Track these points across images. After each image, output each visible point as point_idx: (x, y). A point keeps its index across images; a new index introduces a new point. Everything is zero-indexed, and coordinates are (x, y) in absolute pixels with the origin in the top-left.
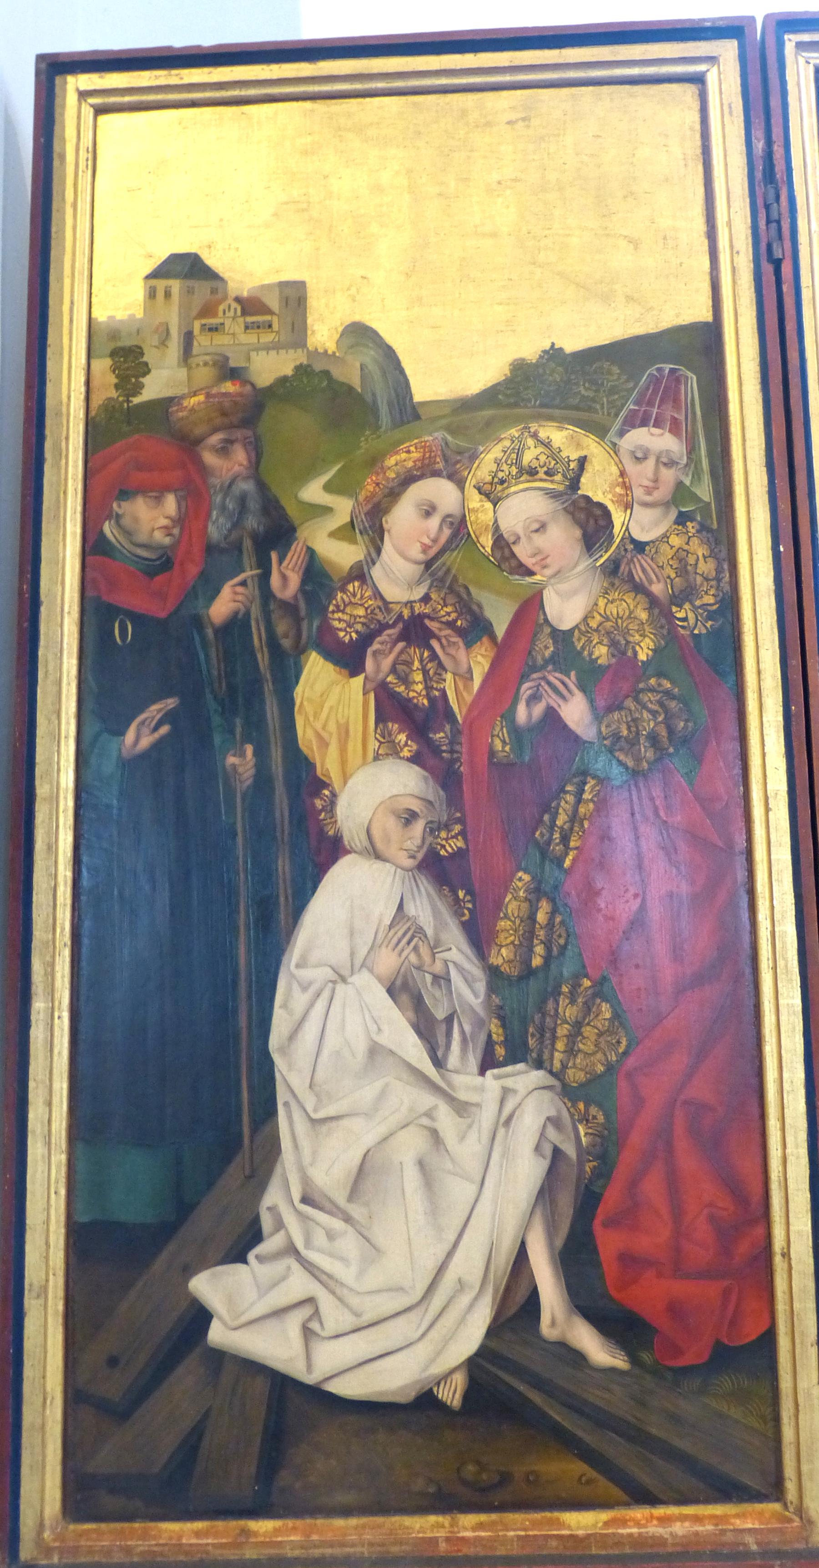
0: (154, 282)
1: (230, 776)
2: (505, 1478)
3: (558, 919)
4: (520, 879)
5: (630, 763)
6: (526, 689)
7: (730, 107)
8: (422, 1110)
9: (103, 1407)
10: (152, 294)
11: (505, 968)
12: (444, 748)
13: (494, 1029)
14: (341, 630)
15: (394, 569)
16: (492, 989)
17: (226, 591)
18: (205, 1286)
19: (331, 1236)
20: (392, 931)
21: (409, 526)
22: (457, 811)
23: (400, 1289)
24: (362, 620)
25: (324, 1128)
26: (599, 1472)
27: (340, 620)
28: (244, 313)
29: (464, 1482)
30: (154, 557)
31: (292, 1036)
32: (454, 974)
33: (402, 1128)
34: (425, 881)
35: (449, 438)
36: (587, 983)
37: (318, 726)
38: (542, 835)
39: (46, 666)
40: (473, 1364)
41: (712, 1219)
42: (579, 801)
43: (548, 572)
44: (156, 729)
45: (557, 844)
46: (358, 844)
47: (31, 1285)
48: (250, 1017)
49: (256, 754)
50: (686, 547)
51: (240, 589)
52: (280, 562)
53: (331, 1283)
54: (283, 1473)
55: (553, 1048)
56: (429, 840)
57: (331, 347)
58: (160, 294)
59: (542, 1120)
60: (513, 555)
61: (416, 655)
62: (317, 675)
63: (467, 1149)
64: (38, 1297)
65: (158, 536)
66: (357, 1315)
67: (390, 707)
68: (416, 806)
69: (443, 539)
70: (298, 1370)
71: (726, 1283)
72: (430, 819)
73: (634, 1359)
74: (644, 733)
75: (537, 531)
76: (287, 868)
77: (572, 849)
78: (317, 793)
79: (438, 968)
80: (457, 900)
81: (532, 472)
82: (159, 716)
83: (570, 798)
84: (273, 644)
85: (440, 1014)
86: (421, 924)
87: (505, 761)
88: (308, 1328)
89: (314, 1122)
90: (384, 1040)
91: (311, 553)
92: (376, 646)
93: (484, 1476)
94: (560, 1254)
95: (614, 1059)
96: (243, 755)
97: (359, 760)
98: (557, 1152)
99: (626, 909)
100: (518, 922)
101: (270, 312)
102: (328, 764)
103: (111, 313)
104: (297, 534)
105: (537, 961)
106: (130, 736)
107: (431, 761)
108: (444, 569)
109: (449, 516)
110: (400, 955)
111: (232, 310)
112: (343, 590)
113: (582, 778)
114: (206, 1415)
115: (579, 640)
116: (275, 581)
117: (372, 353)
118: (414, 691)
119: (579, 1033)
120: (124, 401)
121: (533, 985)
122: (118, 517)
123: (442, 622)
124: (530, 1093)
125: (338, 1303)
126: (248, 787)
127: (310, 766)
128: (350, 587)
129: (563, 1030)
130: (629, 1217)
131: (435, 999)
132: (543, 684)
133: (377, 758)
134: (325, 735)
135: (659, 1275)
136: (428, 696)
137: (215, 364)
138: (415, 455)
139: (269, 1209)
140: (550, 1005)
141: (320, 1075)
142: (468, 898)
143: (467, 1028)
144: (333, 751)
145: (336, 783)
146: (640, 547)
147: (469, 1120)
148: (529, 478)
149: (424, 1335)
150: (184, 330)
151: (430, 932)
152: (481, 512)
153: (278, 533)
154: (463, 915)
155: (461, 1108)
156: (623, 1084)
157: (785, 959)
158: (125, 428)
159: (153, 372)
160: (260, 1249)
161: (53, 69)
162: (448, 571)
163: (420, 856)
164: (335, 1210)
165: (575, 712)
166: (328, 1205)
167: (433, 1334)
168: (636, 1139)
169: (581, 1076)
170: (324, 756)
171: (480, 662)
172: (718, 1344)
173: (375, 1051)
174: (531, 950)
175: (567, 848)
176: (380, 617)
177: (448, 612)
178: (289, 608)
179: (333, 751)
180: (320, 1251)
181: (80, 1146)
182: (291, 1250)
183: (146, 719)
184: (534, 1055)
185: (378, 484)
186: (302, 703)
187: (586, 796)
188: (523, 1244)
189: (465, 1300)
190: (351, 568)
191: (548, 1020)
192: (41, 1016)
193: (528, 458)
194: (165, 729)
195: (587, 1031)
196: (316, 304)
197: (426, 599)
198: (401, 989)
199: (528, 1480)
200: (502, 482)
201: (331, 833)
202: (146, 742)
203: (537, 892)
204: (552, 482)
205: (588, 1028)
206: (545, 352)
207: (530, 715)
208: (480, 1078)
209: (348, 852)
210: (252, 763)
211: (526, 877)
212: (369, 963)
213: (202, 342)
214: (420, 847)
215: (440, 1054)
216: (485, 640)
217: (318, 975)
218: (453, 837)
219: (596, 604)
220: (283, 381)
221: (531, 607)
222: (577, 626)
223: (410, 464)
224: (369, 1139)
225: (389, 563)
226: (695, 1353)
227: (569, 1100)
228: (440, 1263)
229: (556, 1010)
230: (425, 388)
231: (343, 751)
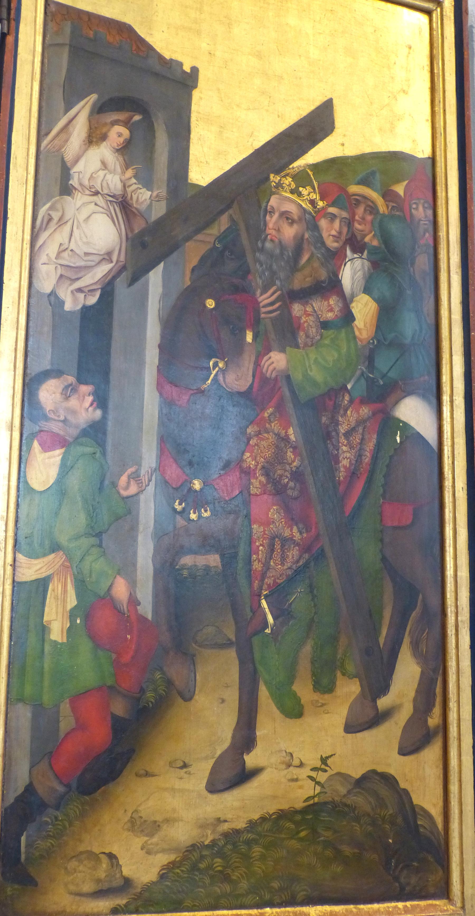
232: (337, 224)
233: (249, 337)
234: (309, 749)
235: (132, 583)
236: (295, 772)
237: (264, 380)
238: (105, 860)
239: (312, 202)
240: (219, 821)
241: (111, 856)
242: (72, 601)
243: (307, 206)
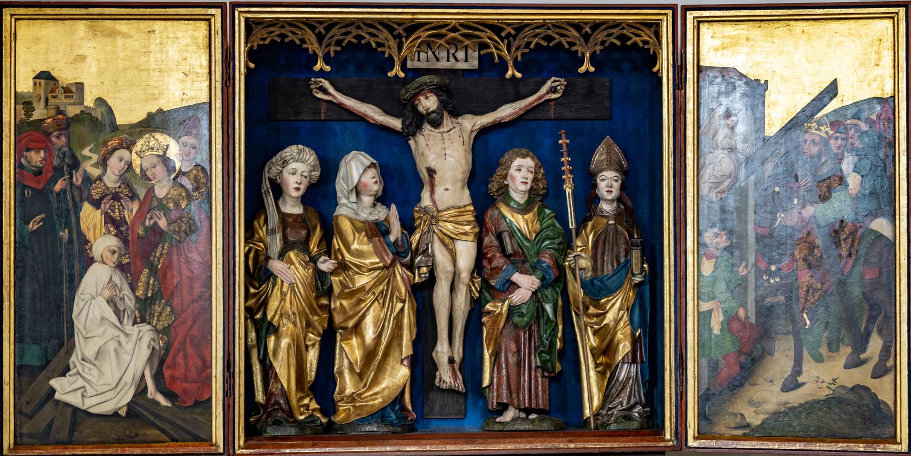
2: (137, 435)
10: (35, 84)
18: (53, 383)
19: (90, 370)
21: (115, 164)
40: (129, 405)
57: (92, 105)
61: (116, 203)
62: (87, 209)
63: (128, 346)
68: (116, 249)
70: (80, 406)
81: (152, 149)
84: (73, 199)
90: (105, 316)
91: (85, 171)
106: (31, 225)
116: (74, 179)
146: (184, 174)
152: (136, 161)
153: (75, 164)
155: (127, 335)
173: (103, 319)
182: (78, 373)
198: (111, 301)
202: (35, 227)
213: (51, 101)
217: (87, 297)
221: (151, 191)
224: (101, 343)
226: (190, 403)
232: (839, 141)
233: (796, 201)
234: (827, 375)
235: (746, 311)
236: (820, 385)
237: (803, 219)
238: (739, 416)
239: (827, 133)
240: (786, 403)
241: (742, 415)
242: (722, 318)
243: (824, 135)
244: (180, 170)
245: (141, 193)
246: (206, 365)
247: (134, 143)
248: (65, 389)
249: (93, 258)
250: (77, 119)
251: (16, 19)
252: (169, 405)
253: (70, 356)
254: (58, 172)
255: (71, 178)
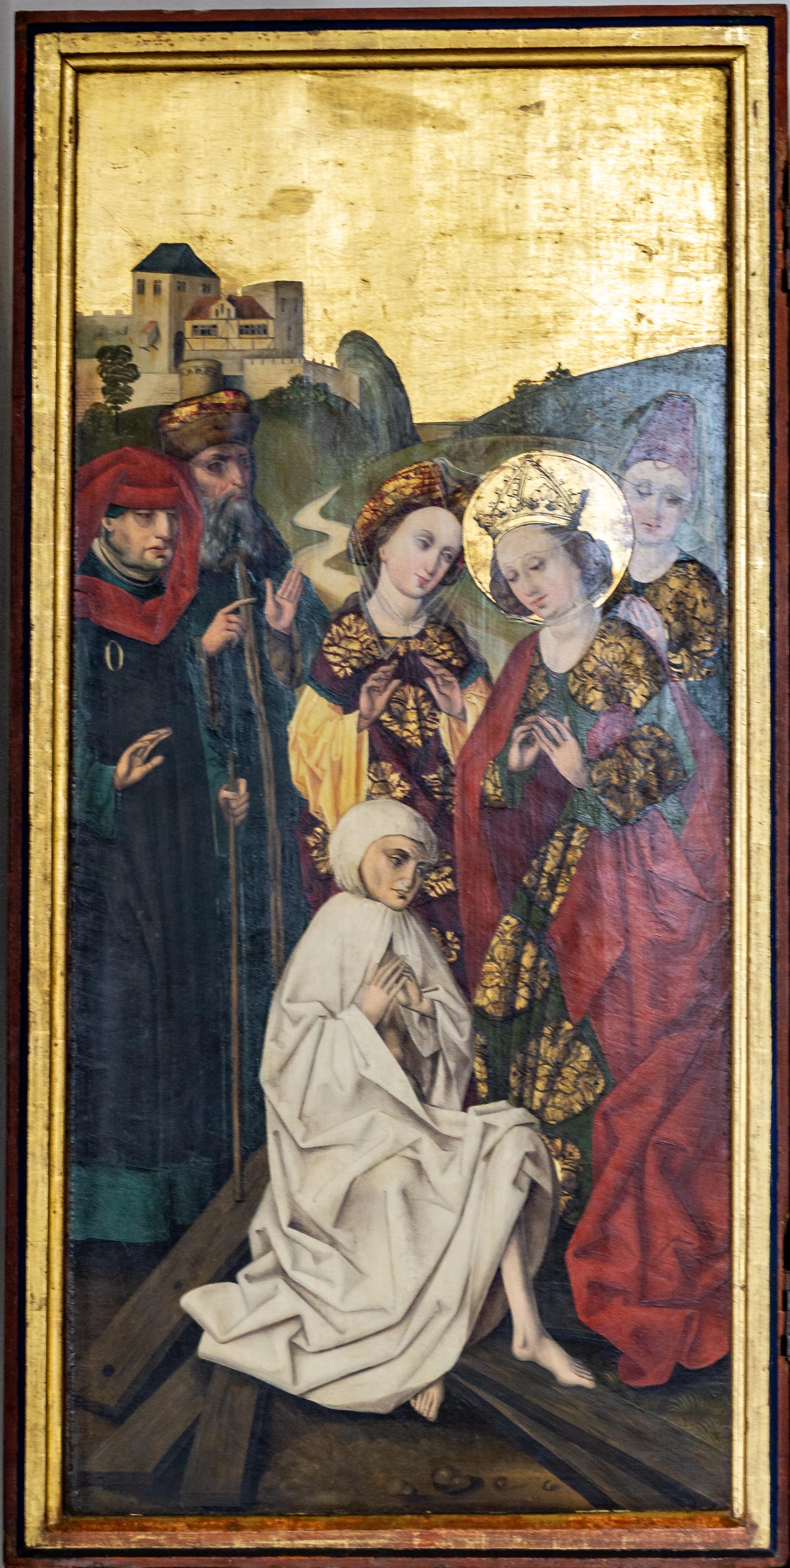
0: (142, 275)
1: (222, 810)
2: (476, 1483)
3: (543, 963)
4: (507, 923)
5: (620, 812)
6: (518, 734)
7: (755, 107)
8: (407, 1142)
9: (102, 1412)
10: (140, 288)
11: (490, 1009)
12: (437, 789)
13: (477, 1067)
14: (336, 664)
15: (390, 602)
16: (476, 1028)
17: (220, 619)
18: (196, 1302)
19: (317, 1258)
20: (382, 969)
21: (407, 556)
22: (448, 853)
23: (382, 1309)
24: (357, 655)
25: (313, 1157)
26: (562, 1479)
27: (335, 654)
28: (240, 315)
29: (437, 1486)
30: (145, 579)
31: (282, 1069)
32: (441, 1014)
33: (388, 1158)
34: (414, 922)
35: (450, 464)
36: (568, 1026)
37: (311, 762)
38: (530, 880)
39: (39, 693)
40: (448, 1380)
41: (677, 1252)
42: (567, 847)
43: (545, 612)
44: (148, 760)
45: (544, 890)
46: (349, 882)
47: (32, 1296)
48: (241, 1049)
49: (249, 789)
50: (686, 590)
51: (233, 618)
52: (275, 592)
53: (317, 1303)
54: (268, 1474)
55: (534, 1088)
56: (419, 880)
57: (330, 359)
58: (149, 289)
59: (520, 1155)
60: (511, 594)
61: (410, 692)
62: (311, 708)
63: (448, 1179)
64: (40, 1308)
65: (149, 556)
66: (341, 1332)
67: (386, 746)
68: (407, 846)
69: (441, 573)
70: (284, 1382)
71: (688, 1312)
72: (421, 860)
73: (599, 1379)
74: (634, 781)
75: (536, 568)
76: (279, 904)
77: (559, 895)
78: (309, 831)
79: (425, 1006)
80: (445, 942)
82: (152, 746)
83: (559, 845)
85: (426, 1051)
86: (410, 964)
87: (497, 804)
88: (295, 1344)
89: (302, 1150)
91: (305, 582)
92: (370, 683)
93: (456, 1481)
94: (535, 1279)
95: (592, 1099)
96: (235, 789)
97: (352, 799)
98: (534, 1186)
99: (610, 956)
100: (504, 964)
101: (265, 316)
102: (321, 802)
103: (97, 308)
104: (292, 562)
105: (521, 1004)
106: (122, 767)
107: (423, 803)
108: (441, 605)
109: (447, 548)
110: (388, 992)
111: (226, 312)
112: (339, 622)
113: (570, 824)
114: (197, 1421)
115: (574, 684)
116: (269, 609)
117: (371, 366)
118: (408, 730)
119: (559, 1074)
120: (112, 408)
121: (517, 1026)
122: (108, 534)
123: (438, 661)
124: (510, 1129)
125: (322, 1320)
126: (242, 822)
127: (304, 803)
128: (346, 620)
129: (543, 1071)
130: (601, 1247)
131: (421, 1035)
132: (536, 728)
133: (370, 797)
134: (318, 771)
135: (626, 1302)
136: (422, 737)
137: (208, 370)
138: (415, 481)
139: (258, 1232)
140: (533, 1044)
141: (309, 1108)
142: (456, 939)
143: (452, 1065)
144: (326, 787)
145: (329, 822)
147: (451, 1153)
148: (529, 511)
149: (403, 1352)
150: (174, 331)
151: (418, 971)
152: (480, 550)
153: (273, 560)
154: (451, 956)
155: (443, 1141)
156: (599, 1124)
157: (758, 1010)
158: (113, 437)
159: (143, 376)
160: (250, 1269)
161: (31, 26)
162: (445, 608)
163: (410, 896)
164: (321, 1235)
165: (567, 760)
166: (315, 1230)
167: (411, 1351)
168: (611, 1175)
169: (560, 1115)
170: (317, 793)
171: (473, 702)
172: (679, 1366)
173: (362, 1084)
174: (515, 992)
175: (554, 894)
176: (375, 652)
177: (444, 651)
178: (286, 639)
179: (326, 787)
180: (306, 1272)
181: (74, 1172)
182: (279, 1271)
183: (138, 749)
184: (515, 1093)
185: (375, 510)
186: (295, 739)
187: (575, 843)
188: (499, 1271)
189: (442, 1321)
190: (347, 600)
191: (530, 1060)
192: (40, 1043)
193: (528, 492)
194: (157, 760)
195: (566, 1071)
196: (314, 309)
197: (422, 635)
198: (390, 1026)
199: (497, 1486)
200: (503, 514)
201: (323, 870)
202: (138, 773)
203: (521, 937)
204: (553, 516)
205: (568, 1069)
206: (552, 374)
207: (522, 761)
208: (463, 1113)
209: (339, 890)
210: (245, 798)
211: (513, 921)
212: (357, 1000)
213: (195, 345)
214: (410, 888)
215: (425, 1089)
216: (480, 681)
217: (309, 1010)
218: (443, 879)
219: (592, 648)
220: (279, 393)
221: (527, 648)
222: (572, 671)
223: (408, 491)
224: (356, 1168)
225: (386, 597)
226: (656, 1375)
227: (548, 1137)
228: (419, 1287)
229: (538, 1051)
230: (428, 406)
231: (336, 788)
244: (627, 579)
245: (496, 655)
246: (713, 1243)
247: (470, 486)
248: (231, 1324)
249: (329, 877)
250: (279, 405)
251: (79, 71)
252: (587, 1381)
253: (251, 1211)
254: (215, 588)
255: (260, 604)
